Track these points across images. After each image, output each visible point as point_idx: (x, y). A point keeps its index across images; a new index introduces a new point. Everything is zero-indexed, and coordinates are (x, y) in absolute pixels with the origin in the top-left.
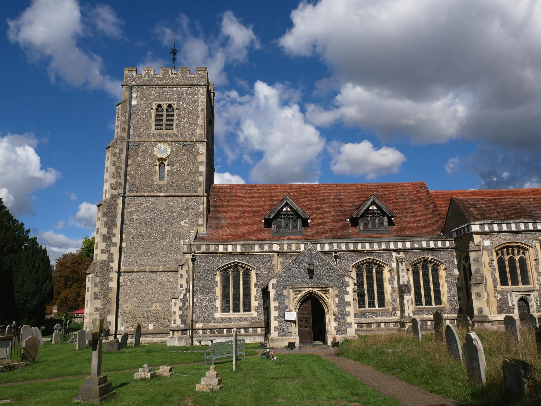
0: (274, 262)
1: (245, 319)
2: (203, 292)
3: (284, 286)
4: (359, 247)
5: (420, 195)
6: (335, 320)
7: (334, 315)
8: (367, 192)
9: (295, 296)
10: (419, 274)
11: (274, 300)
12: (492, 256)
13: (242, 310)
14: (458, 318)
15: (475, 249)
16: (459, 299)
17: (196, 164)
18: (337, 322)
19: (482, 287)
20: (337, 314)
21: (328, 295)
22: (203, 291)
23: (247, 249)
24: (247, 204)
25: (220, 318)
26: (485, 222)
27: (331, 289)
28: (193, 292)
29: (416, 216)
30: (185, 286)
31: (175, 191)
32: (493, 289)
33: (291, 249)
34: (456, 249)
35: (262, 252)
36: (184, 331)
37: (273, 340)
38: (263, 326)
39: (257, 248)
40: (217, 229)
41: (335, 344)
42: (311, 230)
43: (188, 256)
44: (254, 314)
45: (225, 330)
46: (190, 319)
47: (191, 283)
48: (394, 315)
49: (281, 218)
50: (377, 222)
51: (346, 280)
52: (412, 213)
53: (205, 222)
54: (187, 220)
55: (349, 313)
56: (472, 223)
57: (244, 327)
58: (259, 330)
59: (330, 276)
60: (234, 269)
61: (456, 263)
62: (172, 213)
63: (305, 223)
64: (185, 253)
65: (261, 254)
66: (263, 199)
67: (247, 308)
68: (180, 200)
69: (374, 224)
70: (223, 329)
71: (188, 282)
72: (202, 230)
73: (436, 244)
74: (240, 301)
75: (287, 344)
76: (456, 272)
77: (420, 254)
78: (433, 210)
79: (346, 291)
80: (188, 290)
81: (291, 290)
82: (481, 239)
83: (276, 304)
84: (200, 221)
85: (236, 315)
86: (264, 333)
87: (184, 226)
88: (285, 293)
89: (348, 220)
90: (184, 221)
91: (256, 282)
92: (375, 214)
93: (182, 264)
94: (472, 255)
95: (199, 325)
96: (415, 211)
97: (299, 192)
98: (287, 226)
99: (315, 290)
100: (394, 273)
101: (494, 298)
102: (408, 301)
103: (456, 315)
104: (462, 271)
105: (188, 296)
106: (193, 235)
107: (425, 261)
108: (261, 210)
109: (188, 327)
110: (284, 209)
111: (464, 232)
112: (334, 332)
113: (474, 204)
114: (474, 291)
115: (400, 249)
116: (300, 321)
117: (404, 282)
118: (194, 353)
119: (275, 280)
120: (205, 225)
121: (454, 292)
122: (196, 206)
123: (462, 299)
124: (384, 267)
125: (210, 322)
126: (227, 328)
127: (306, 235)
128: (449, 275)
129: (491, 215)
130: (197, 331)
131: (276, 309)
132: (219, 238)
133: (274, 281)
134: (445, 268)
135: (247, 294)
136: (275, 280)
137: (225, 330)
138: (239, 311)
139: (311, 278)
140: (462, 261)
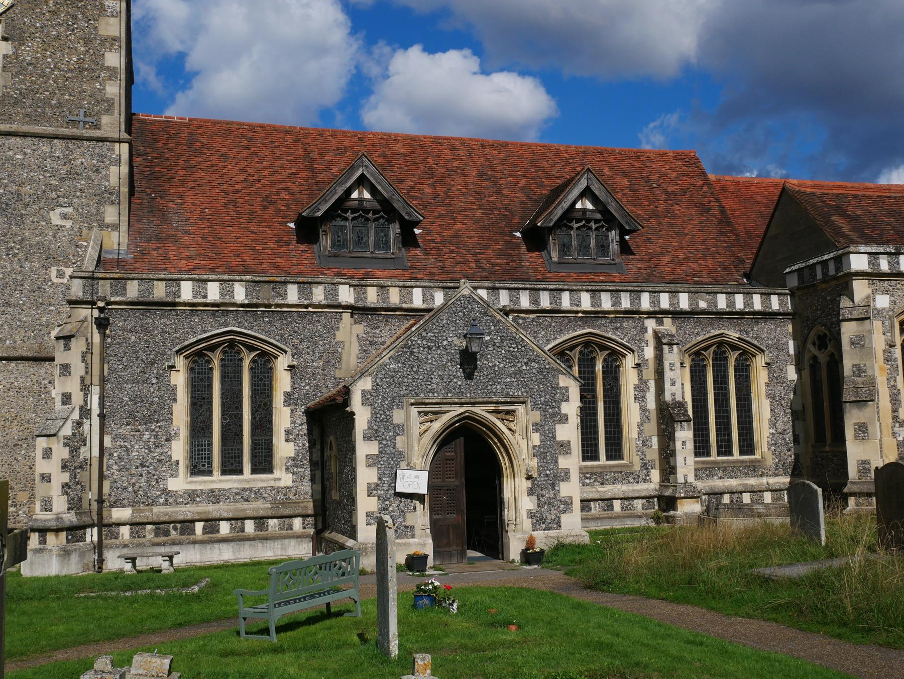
0: (340, 336)
2: (131, 418)
3: (393, 399)
4: (566, 301)
5: (686, 183)
6: (530, 492)
7: (529, 478)
8: (558, 167)
9: (423, 428)
10: (705, 376)
11: (367, 438)
12: (893, 335)
13: (247, 467)
14: (792, 489)
15: (856, 314)
16: (796, 440)
17: (95, 45)
18: (535, 498)
19: (870, 409)
20: (535, 475)
21: (512, 425)
22: (131, 415)
23: (265, 295)
24: (241, 177)
25: (185, 492)
26: (881, 250)
27: (520, 409)
28: (102, 416)
29: (681, 235)
30: (77, 399)
31: (30, 118)
32: (890, 414)
33: (386, 300)
35: (306, 306)
36: (75, 531)
38: (310, 511)
39: (293, 295)
40: (159, 239)
41: (530, 556)
42: (426, 254)
43: (84, 312)
44: (282, 478)
45: (199, 526)
46: (92, 495)
47: (96, 390)
48: (645, 480)
49: (346, 219)
50: (593, 242)
51: (561, 384)
52: (671, 225)
53: (125, 218)
54: (69, 210)
55: (567, 472)
56: (852, 249)
57: (255, 514)
58: (297, 523)
59: (519, 372)
60: (224, 352)
61: (792, 352)
62: (22, 184)
63: (408, 240)
64: (75, 303)
67: (263, 462)
68: (46, 149)
69: (584, 248)
70: (193, 521)
71: (85, 388)
72: (117, 241)
74: (241, 443)
76: (792, 374)
77: (712, 325)
78: (720, 222)
79: (559, 413)
80: (85, 412)
81: (414, 410)
82: (869, 291)
83: (373, 448)
84: (110, 214)
85: (231, 482)
86: (311, 531)
87: (60, 228)
88: (398, 416)
89: (518, 234)
90: (59, 210)
91: (288, 389)
92: (588, 221)
93: (66, 333)
94: (848, 330)
95: (120, 514)
96: (679, 221)
97: (383, 155)
98: (360, 241)
99: (477, 409)
100: (649, 374)
101: (891, 438)
102: (684, 443)
103: (786, 480)
104: (806, 373)
105: (86, 427)
106: (91, 254)
107: (721, 344)
108: (284, 195)
109: (86, 520)
110: (355, 195)
111: (825, 274)
112: (527, 524)
113: (837, 206)
114: (852, 418)
115: (665, 312)
116: (436, 496)
117: (673, 395)
118: (159, 598)
119: (369, 379)
120: (124, 227)
121: (785, 422)
122: (97, 171)
123: (801, 440)
124: (624, 356)
125: (153, 502)
126: (206, 520)
127: (412, 267)
128: (775, 380)
129: (881, 235)
130: (113, 528)
131: (372, 461)
132: (168, 265)
133: (366, 384)
134: (768, 364)
136: (369, 379)
137: (199, 526)
138: (240, 472)
139: (469, 376)
140: (810, 347)
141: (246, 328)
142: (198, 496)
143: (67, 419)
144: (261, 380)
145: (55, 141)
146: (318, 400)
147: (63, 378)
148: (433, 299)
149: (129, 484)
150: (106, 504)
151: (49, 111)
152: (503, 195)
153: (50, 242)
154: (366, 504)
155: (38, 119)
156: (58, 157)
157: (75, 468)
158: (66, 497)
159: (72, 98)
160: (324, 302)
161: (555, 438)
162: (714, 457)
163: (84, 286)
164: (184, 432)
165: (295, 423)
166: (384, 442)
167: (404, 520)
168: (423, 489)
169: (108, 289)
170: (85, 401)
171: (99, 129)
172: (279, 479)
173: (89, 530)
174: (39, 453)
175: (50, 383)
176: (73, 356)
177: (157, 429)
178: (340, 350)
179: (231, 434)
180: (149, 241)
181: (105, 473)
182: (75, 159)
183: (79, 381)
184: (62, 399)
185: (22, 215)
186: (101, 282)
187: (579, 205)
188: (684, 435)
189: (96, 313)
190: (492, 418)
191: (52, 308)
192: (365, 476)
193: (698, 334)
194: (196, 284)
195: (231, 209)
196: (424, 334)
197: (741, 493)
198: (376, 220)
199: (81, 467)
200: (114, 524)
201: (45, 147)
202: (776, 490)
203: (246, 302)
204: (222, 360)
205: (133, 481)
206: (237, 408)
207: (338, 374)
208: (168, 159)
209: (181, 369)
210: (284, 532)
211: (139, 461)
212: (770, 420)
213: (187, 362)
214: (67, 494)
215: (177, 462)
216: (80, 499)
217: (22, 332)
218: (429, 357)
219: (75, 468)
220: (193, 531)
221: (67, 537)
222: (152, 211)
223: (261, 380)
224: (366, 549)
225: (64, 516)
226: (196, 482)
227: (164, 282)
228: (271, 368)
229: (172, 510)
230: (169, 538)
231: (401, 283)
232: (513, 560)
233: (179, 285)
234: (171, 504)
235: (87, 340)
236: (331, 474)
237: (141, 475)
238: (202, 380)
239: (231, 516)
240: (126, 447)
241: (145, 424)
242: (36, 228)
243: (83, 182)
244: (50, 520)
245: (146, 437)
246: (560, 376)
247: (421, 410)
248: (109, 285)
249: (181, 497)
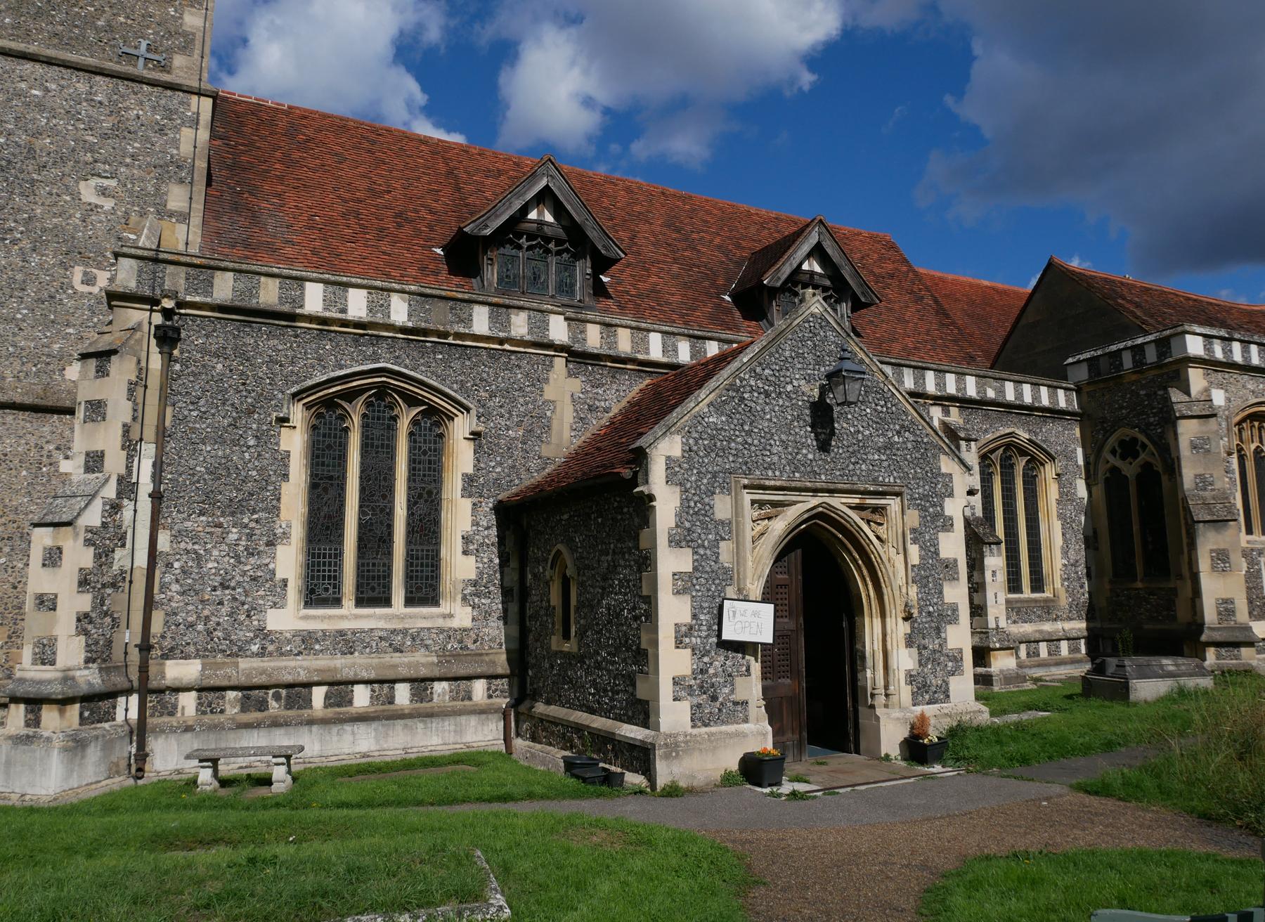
0: (550, 392)
1: (417, 639)
6: (909, 642)
7: (908, 618)
8: (753, 230)
9: (758, 529)
11: (675, 542)
13: (398, 594)
15: (1196, 410)
18: (914, 651)
21: (881, 531)
22: (209, 497)
23: (438, 316)
24: (363, 184)
25: (297, 633)
26: (1214, 332)
27: (893, 504)
28: (156, 497)
30: (115, 462)
34: (1082, 417)
36: (96, 703)
37: (675, 748)
40: (247, 246)
43: (137, 315)
44: (456, 613)
45: (319, 694)
46: (130, 636)
47: (148, 451)
49: (519, 247)
51: (944, 470)
53: (198, 206)
54: (112, 183)
55: (954, 608)
57: (412, 673)
58: (479, 689)
59: (889, 446)
60: (368, 404)
61: (1081, 462)
62: (38, 134)
65: (499, 348)
66: (426, 178)
67: (424, 589)
68: (82, 87)
70: (309, 685)
71: (130, 446)
72: (185, 237)
73: (1036, 397)
75: (731, 762)
78: (937, 313)
80: (127, 487)
81: (747, 497)
84: (177, 198)
88: (722, 507)
89: (727, 298)
90: (94, 182)
91: (470, 470)
99: (837, 502)
104: (1099, 490)
105: (127, 514)
108: (423, 213)
109: (119, 681)
110: (533, 215)
115: (952, 399)
119: (678, 439)
120: (196, 219)
121: (1078, 552)
122: (161, 131)
123: (1093, 574)
125: (240, 651)
126: (330, 684)
128: (1066, 496)
130: (167, 696)
131: (684, 583)
135: (426, 528)
136: (678, 439)
137: (319, 694)
138: (387, 602)
139: (824, 447)
141: (406, 367)
142: (317, 641)
143: (93, 496)
144: (425, 453)
145: (98, 78)
146: (514, 490)
147: (89, 425)
148: (676, 350)
149: (199, 617)
150: (156, 653)
151: (91, 35)
152: (699, 251)
153: (76, 227)
154: (673, 662)
155: (73, 42)
156: (100, 103)
157: (104, 586)
158: (83, 638)
159: (129, 22)
160: (528, 338)
161: (938, 554)
163: (140, 272)
164: (298, 532)
165: (478, 524)
166: (701, 551)
167: (732, 691)
168: (768, 638)
169: (182, 282)
170: (129, 468)
171: (168, 72)
172: (451, 616)
173: (121, 700)
174: (36, 555)
175: (58, 448)
176: (114, 388)
177: (252, 525)
178: (548, 413)
179: (375, 539)
180: (233, 247)
181: (158, 597)
182: (127, 109)
183: (120, 432)
184: (87, 462)
185: (33, 182)
186: (171, 269)
187: (805, 267)
188: (995, 562)
189: (158, 319)
190: (854, 515)
191: (71, 331)
192: (673, 610)
193: (986, 431)
194: (331, 288)
195: (352, 221)
196: (758, 370)
197: (1038, 642)
198: (559, 253)
199: (114, 585)
200: (168, 688)
201: (81, 85)
203: (410, 324)
204: (364, 416)
205: (206, 612)
206: (384, 497)
207: (546, 451)
208: (259, 148)
209: (299, 425)
210: (459, 704)
211: (218, 578)
212: (1062, 548)
213: (307, 414)
214: (86, 633)
215: (285, 582)
216: (109, 643)
217: (17, 365)
219: (104, 586)
220: (308, 703)
221: (81, 714)
222: (236, 207)
223: (425, 453)
224: (677, 745)
225: (78, 673)
226: (314, 617)
227: (278, 281)
228: (441, 436)
229: (272, 664)
230: (266, 713)
231: (634, 324)
232: (887, 756)
233: (302, 288)
234: (271, 654)
235: (139, 362)
236: (550, 610)
237: (221, 603)
238: (329, 447)
239: (373, 676)
240: (196, 552)
241: (233, 514)
242: (55, 204)
243: (136, 145)
244: (50, 682)
245: (233, 537)
246: (942, 457)
248: (183, 275)
249: (289, 642)
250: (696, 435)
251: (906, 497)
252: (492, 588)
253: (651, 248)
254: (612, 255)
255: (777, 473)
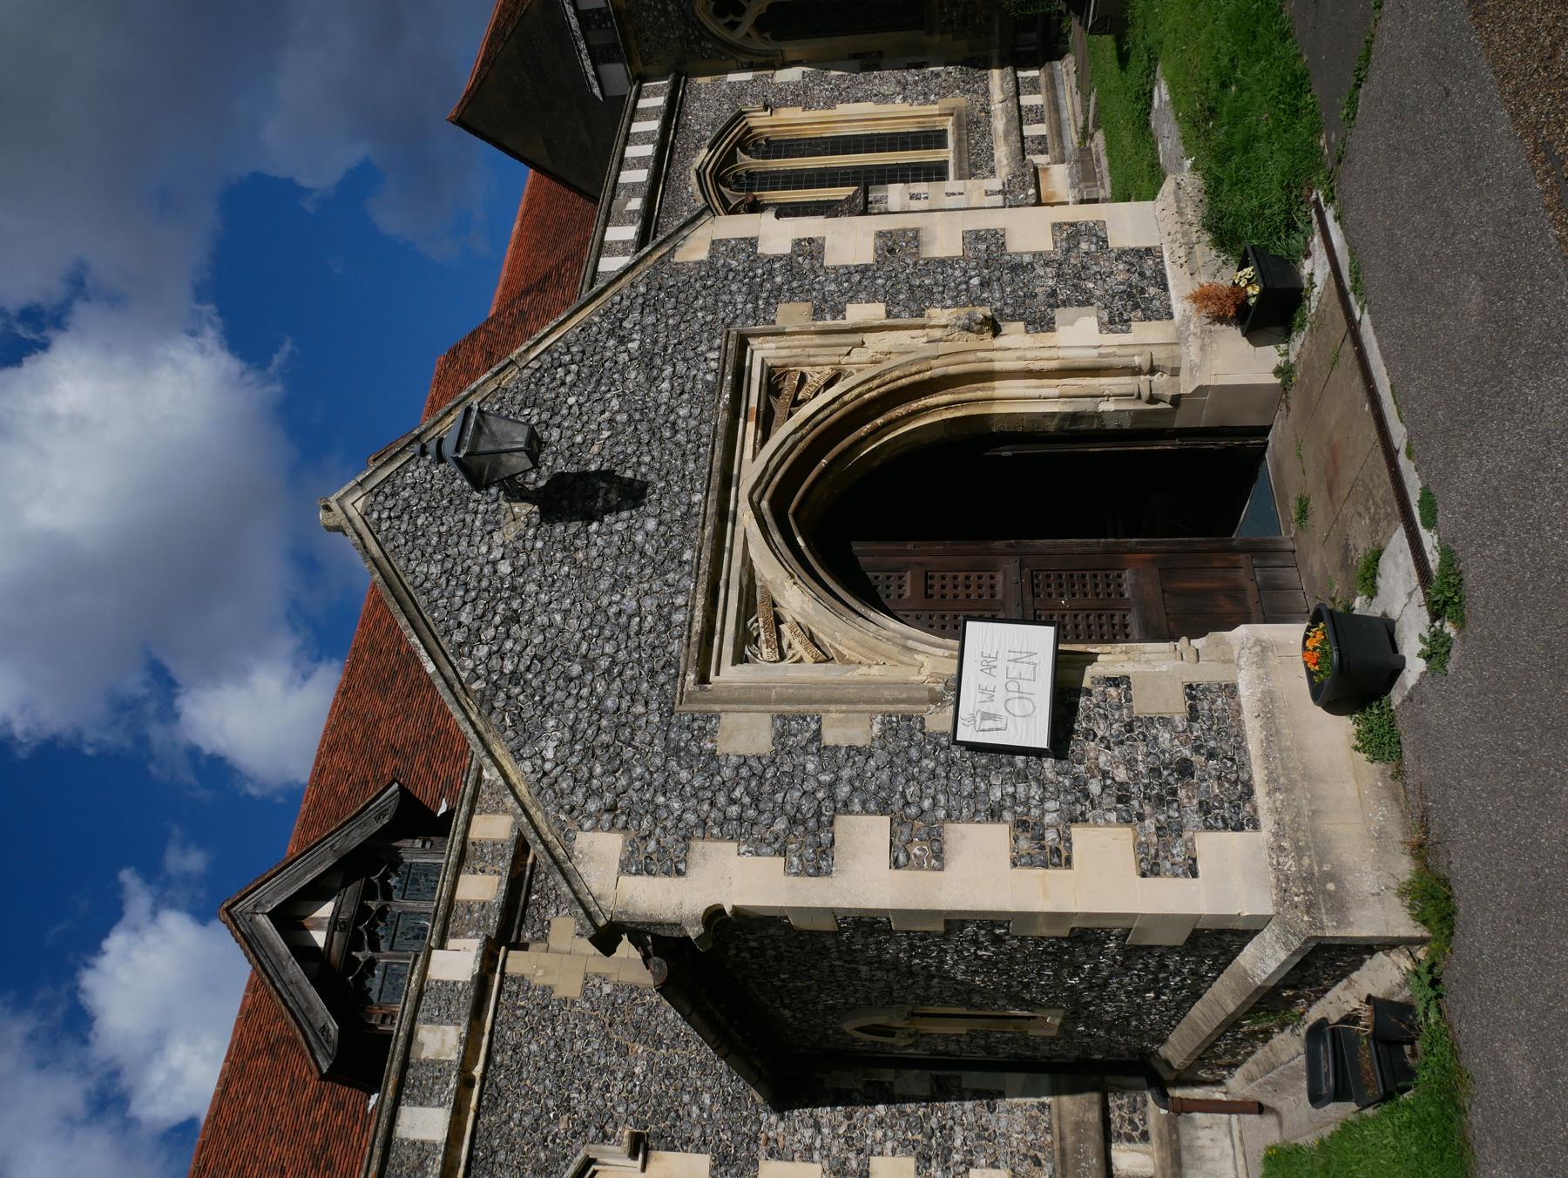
0: (568, 986)
3: (673, 751)
5: (477, 356)
6: (1044, 324)
7: (993, 326)
9: (799, 648)
11: (820, 860)
18: (1060, 314)
21: (816, 377)
27: (763, 352)
35: (466, 1082)
37: (1313, 883)
49: (371, 963)
59: (646, 360)
73: (645, 138)
75: (1333, 734)
76: (792, 75)
78: (542, 291)
81: (729, 674)
83: (865, 838)
88: (745, 736)
99: (750, 469)
104: (791, 49)
108: (318, 1114)
110: (319, 938)
112: (1145, 335)
121: (886, 80)
123: (920, 60)
128: (799, 96)
131: (918, 843)
139: (633, 494)
140: (737, 36)
154: (1102, 877)
160: (463, 1029)
161: (867, 268)
162: (948, 154)
165: (810, 1149)
166: (843, 791)
167: (1166, 722)
168: (1041, 639)
178: (607, 989)
192: (981, 873)
196: (458, 637)
197: (1022, 138)
202: (1018, 88)
212: (878, 102)
218: (542, 619)
224: (1307, 878)
232: (1278, 372)
236: (972, 1035)
246: (680, 257)
247: (728, 650)
250: (580, 793)
251: (750, 326)
252: (934, 1122)
253: (410, 723)
254: (393, 806)
255: (680, 600)
